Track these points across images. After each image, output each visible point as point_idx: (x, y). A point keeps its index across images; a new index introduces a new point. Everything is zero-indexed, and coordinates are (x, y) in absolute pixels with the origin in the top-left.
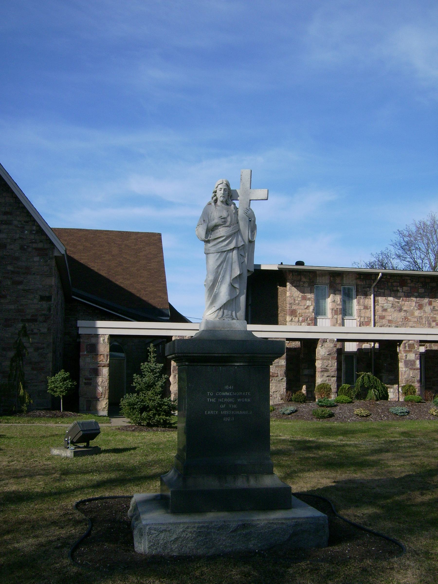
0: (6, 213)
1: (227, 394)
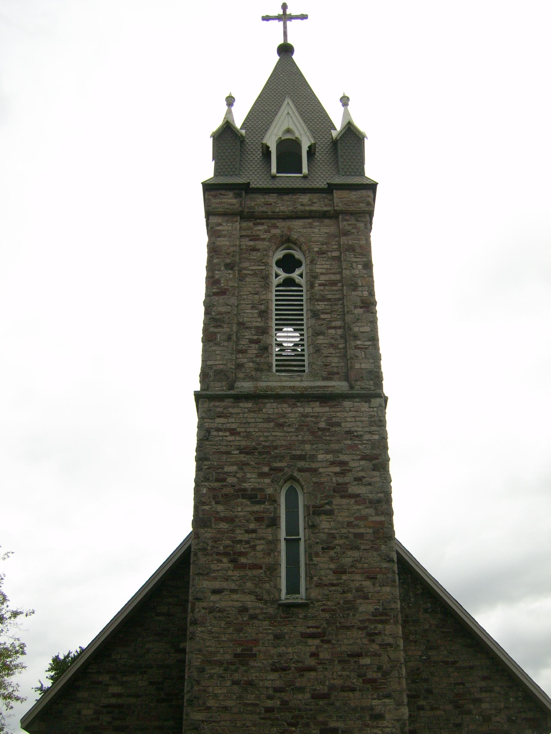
0: (484, 678)
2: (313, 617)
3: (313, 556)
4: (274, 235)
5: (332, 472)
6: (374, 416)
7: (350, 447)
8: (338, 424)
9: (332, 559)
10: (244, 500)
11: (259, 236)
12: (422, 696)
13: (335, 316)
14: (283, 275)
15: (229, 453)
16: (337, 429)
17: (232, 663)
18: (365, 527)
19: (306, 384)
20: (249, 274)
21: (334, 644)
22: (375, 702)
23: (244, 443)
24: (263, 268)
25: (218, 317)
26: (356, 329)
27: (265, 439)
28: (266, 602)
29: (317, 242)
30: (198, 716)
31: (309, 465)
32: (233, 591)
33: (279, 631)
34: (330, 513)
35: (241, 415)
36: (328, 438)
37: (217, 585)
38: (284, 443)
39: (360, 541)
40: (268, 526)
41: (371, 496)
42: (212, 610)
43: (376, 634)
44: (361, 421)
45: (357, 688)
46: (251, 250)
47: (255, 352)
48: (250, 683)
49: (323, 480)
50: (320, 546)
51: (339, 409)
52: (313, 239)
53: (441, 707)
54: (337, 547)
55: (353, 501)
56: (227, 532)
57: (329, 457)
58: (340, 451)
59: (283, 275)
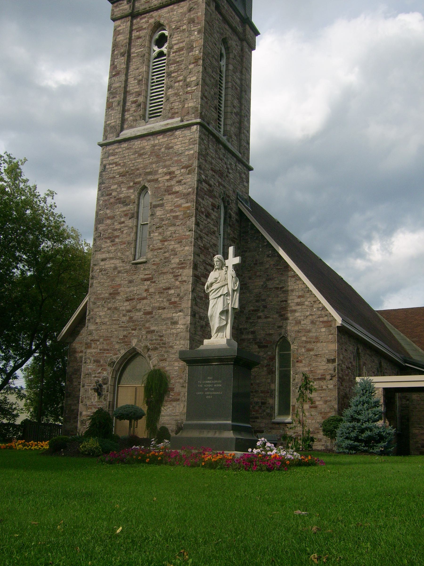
0: (299, 297)
1: (209, 382)
6: (191, 138)
7: (177, 161)
11: (142, 27)
12: (260, 310)
13: (180, 73)
15: (114, 177)
18: (179, 211)
23: (122, 170)
25: (114, 91)
26: (188, 80)
27: (132, 165)
32: (111, 258)
34: (162, 205)
35: (122, 153)
36: (165, 158)
37: (104, 256)
38: (142, 166)
40: (130, 219)
41: (185, 191)
42: (101, 270)
44: (185, 143)
45: (166, 308)
47: (134, 109)
48: (116, 308)
49: (160, 185)
50: (155, 226)
51: (173, 138)
52: (173, 20)
53: (271, 316)
54: (165, 226)
55: (175, 195)
57: (165, 170)
58: (170, 166)
59: (157, 49)
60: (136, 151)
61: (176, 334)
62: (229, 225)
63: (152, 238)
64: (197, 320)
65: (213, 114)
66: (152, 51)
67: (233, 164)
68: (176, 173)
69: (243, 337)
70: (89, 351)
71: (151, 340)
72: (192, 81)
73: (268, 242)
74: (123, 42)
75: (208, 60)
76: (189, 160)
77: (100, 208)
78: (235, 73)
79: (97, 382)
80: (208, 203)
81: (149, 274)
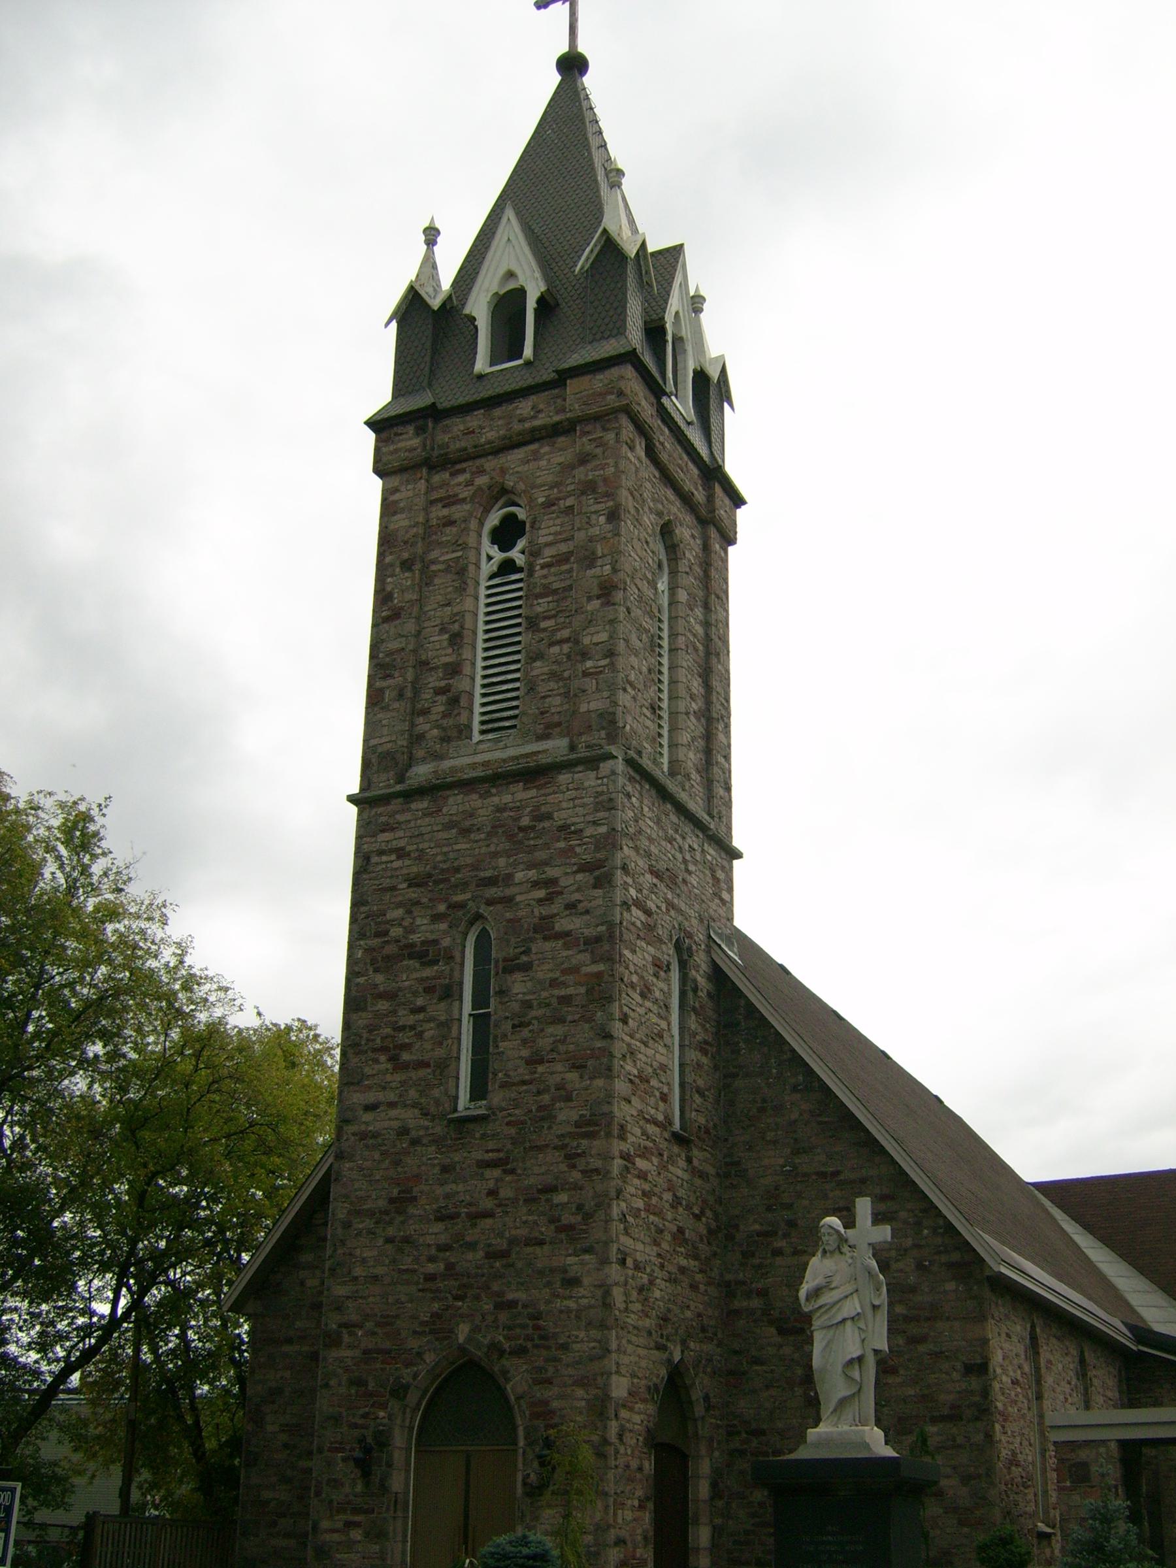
2: (494, 1135)
3: (499, 1039)
4: (480, 489)
5: (534, 900)
7: (565, 853)
8: (549, 816)
9: (525, 1042)
10: (411, 962)
11: (457, 495)
12: (780, 1233)
13: (562, 620)
14: (498, 556)
15: (393, 888)
16: (546, 824)
17: (386, 1213)
19: (512, 752)
20: (439, 570)
21: (520, 1175)
22: (571, 1260)
23: (415, 869)
24: (460, 554)
26: (586, 641)
28: (432, 1121)
29: (542, 486)
30: (341, 1291)
31: (502, 892)
32: (392, 1105)
33: (449, 1160)
34: (527, 967)
35: (412, 824)
36: (532, 842)
37: (371, 1097)
38: (469, 861)
39: (566, 1009)
40: (441, 999)
41: (587, 932)
42: (363, 1136)
43: (579, 1155)
44: (583, 806)
45: (548, 1239)
46: (445, 525)
47: (441, 709)
48: (407, 1240)
49: (521, 913)
50: (510, 1023)
51: (551, 790)
52: (539, 481)
55: (560, 942)
56: (387, 1016)
57: (532, 874)
58: (546, 863)
59: (498, 556)
60: (451, 821)
61: (577, 1311)
62: (694, 1009)
63: (503, 1053)
64: (630, 1272)
65: (648, 723)
66: (484, 558)
67: (696, 846)
68: (563, 882)
69: (737, 1304)
70: (334, 1353)
71: (510, 1328)
72: (597, 644)
73: (793, 1051)
74: (407, 532)
75: (634, 587)
76: (598, 849)
77: (357, 969)
78: (692, 610)
79: (362, 1440)
80: (644, 959)
81: (498, 1151)
